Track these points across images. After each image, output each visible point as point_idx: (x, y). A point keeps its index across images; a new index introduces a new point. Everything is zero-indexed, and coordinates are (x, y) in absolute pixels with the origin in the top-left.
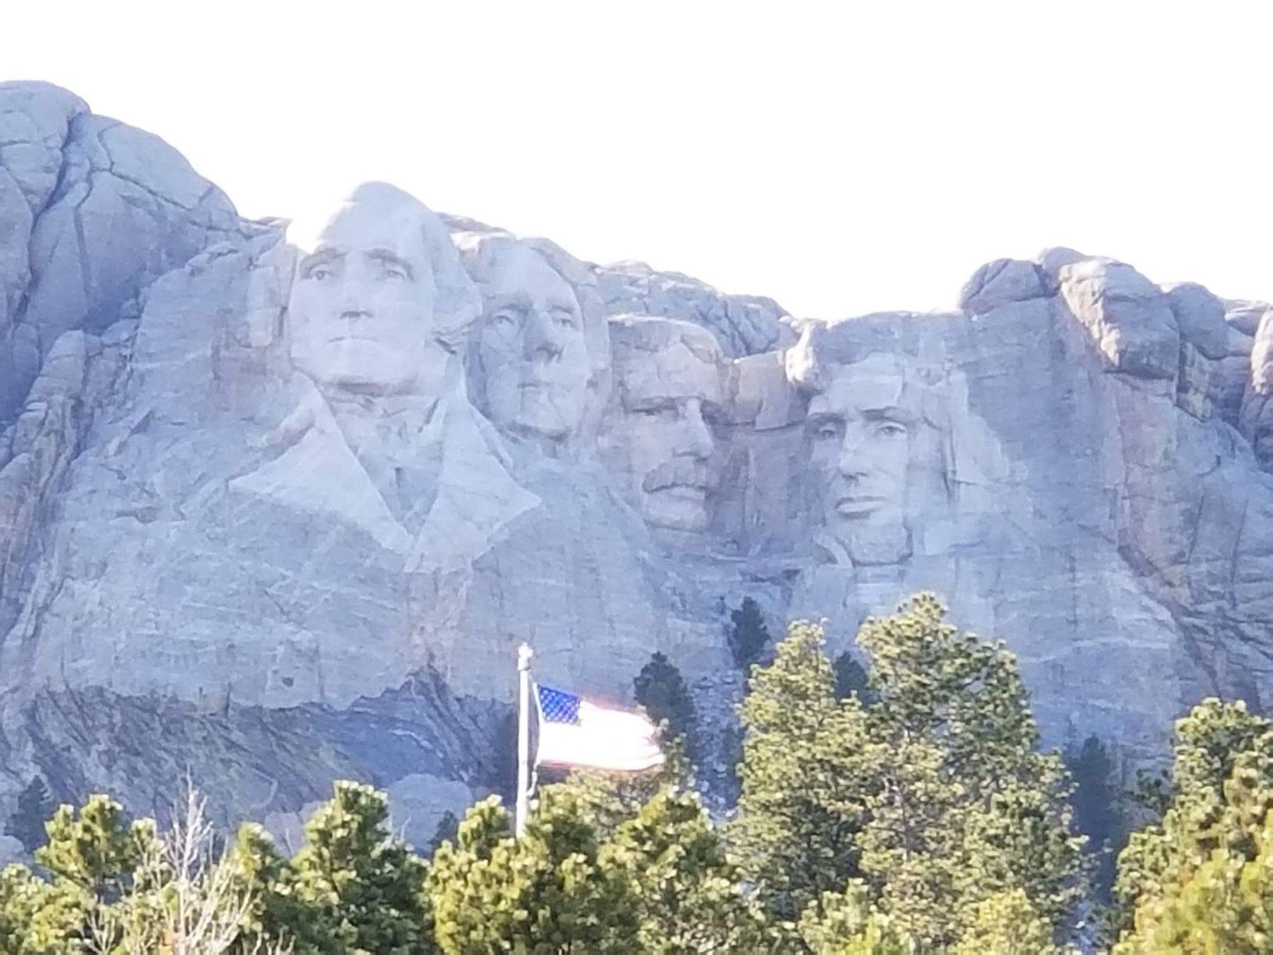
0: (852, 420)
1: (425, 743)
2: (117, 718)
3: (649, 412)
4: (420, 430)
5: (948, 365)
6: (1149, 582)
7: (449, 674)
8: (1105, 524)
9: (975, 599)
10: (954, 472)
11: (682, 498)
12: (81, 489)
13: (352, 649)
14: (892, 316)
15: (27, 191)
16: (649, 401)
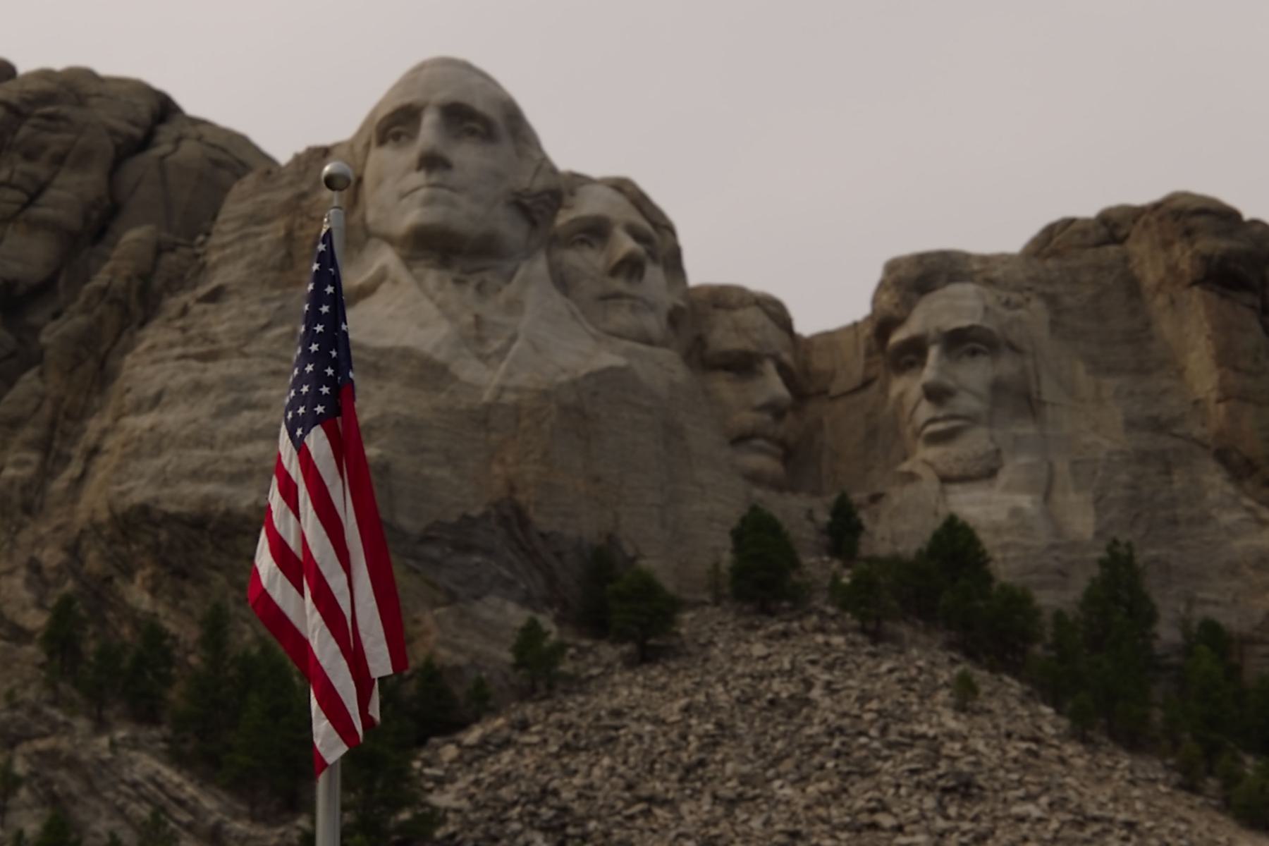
0: (934, 342)
1: (506, 573)
2: (164, 536)
3: (727, 368)
4: (499, 290)
5: (1027, 294)
6: (1248, 485)
7: (531, 510)
8: (1198, 431)
9: (1073, 497)
10: (1039, 393)
11: (761, 450)
12: (141, 348)
13: (427, 471)
14: (967, 257)
15: (113, 132)
16: (726, 354)
